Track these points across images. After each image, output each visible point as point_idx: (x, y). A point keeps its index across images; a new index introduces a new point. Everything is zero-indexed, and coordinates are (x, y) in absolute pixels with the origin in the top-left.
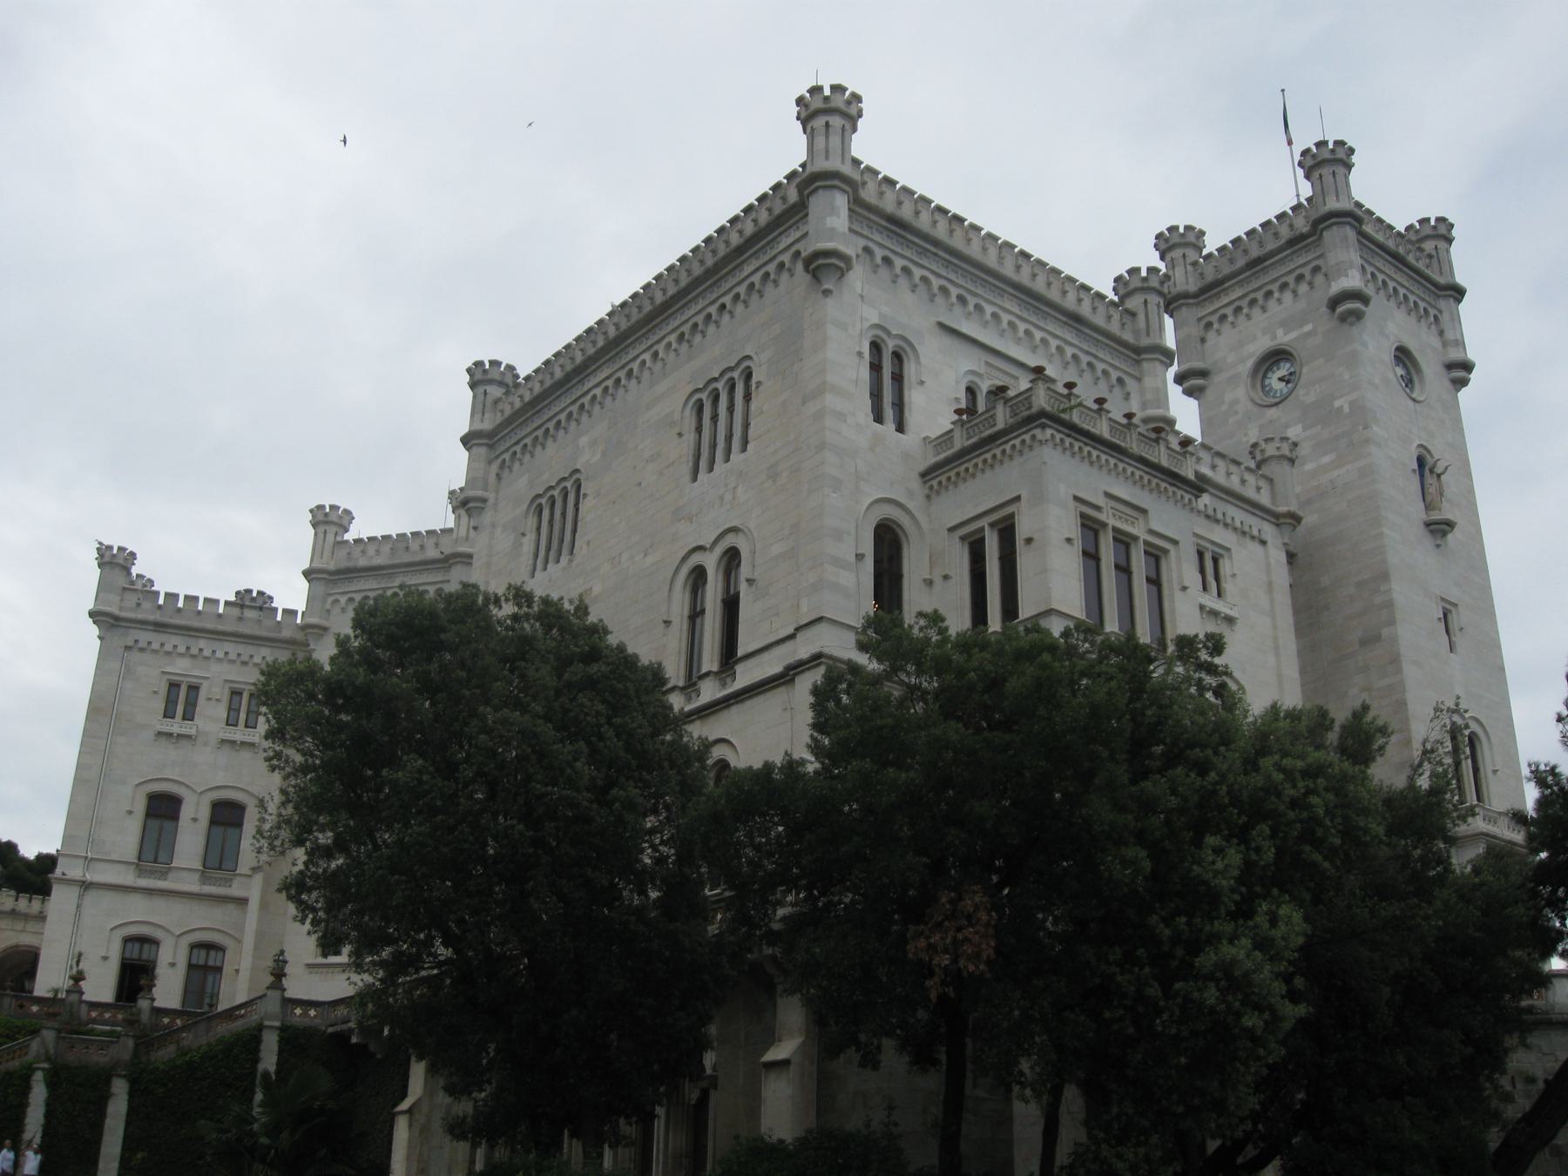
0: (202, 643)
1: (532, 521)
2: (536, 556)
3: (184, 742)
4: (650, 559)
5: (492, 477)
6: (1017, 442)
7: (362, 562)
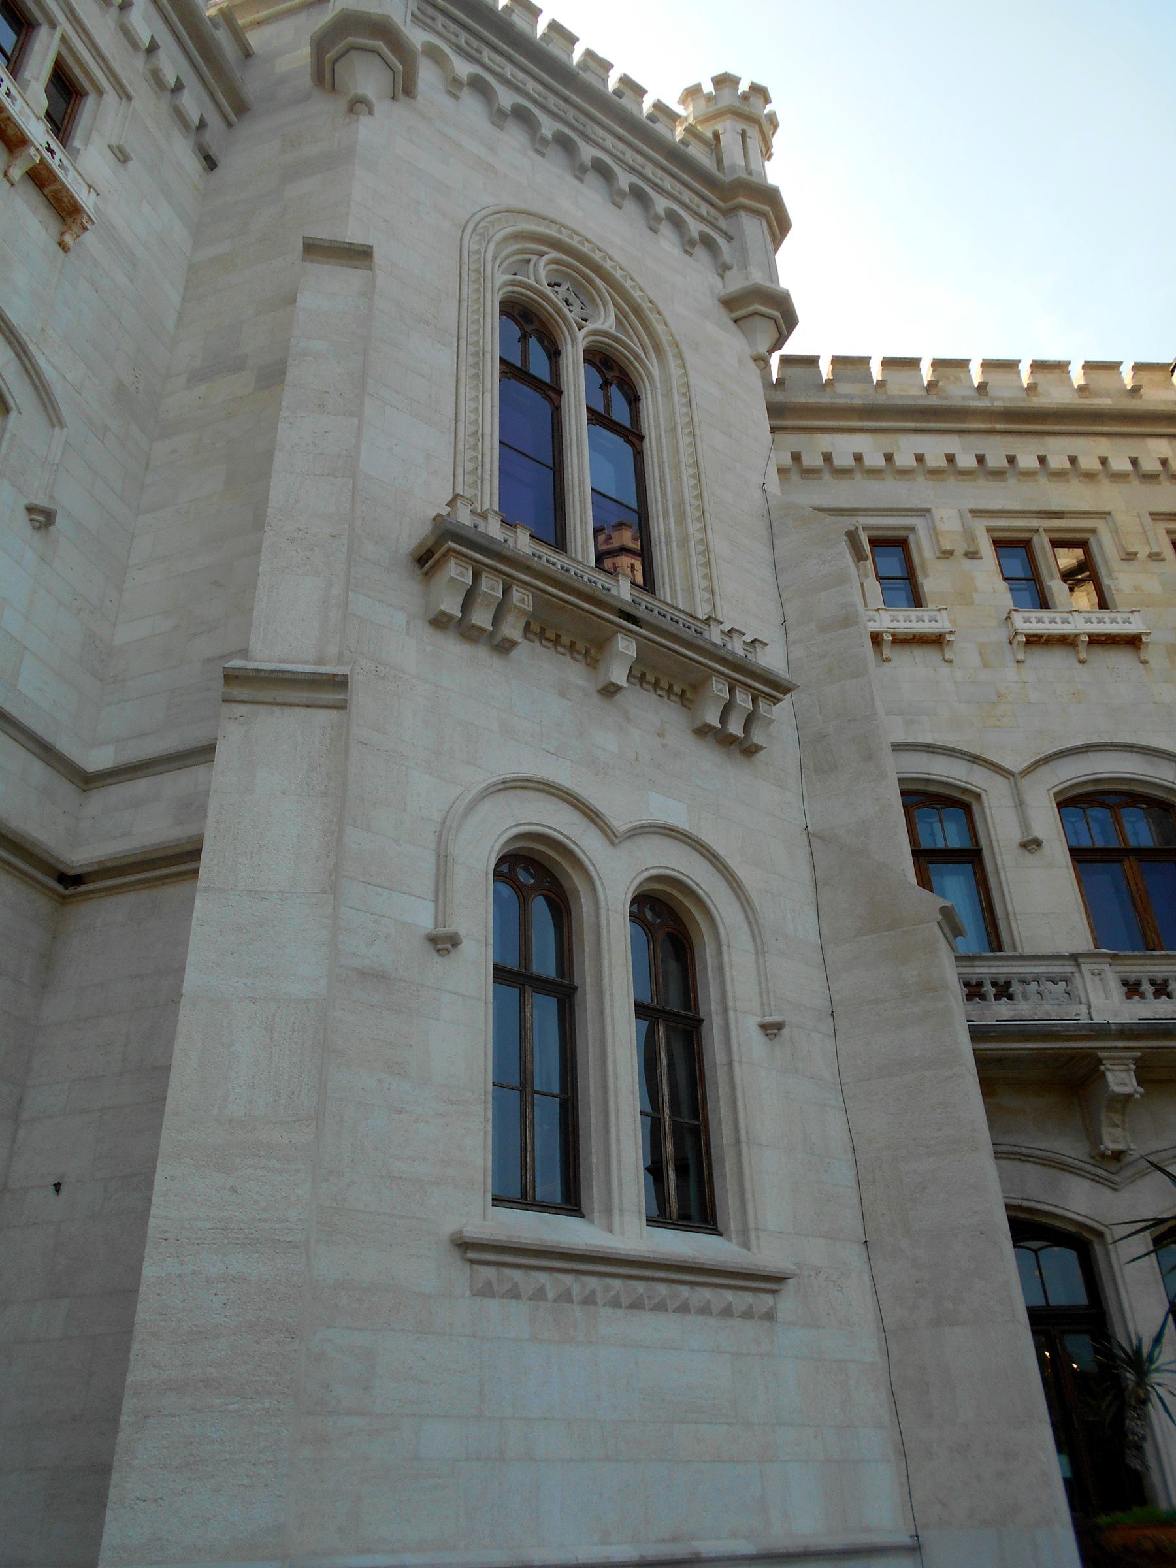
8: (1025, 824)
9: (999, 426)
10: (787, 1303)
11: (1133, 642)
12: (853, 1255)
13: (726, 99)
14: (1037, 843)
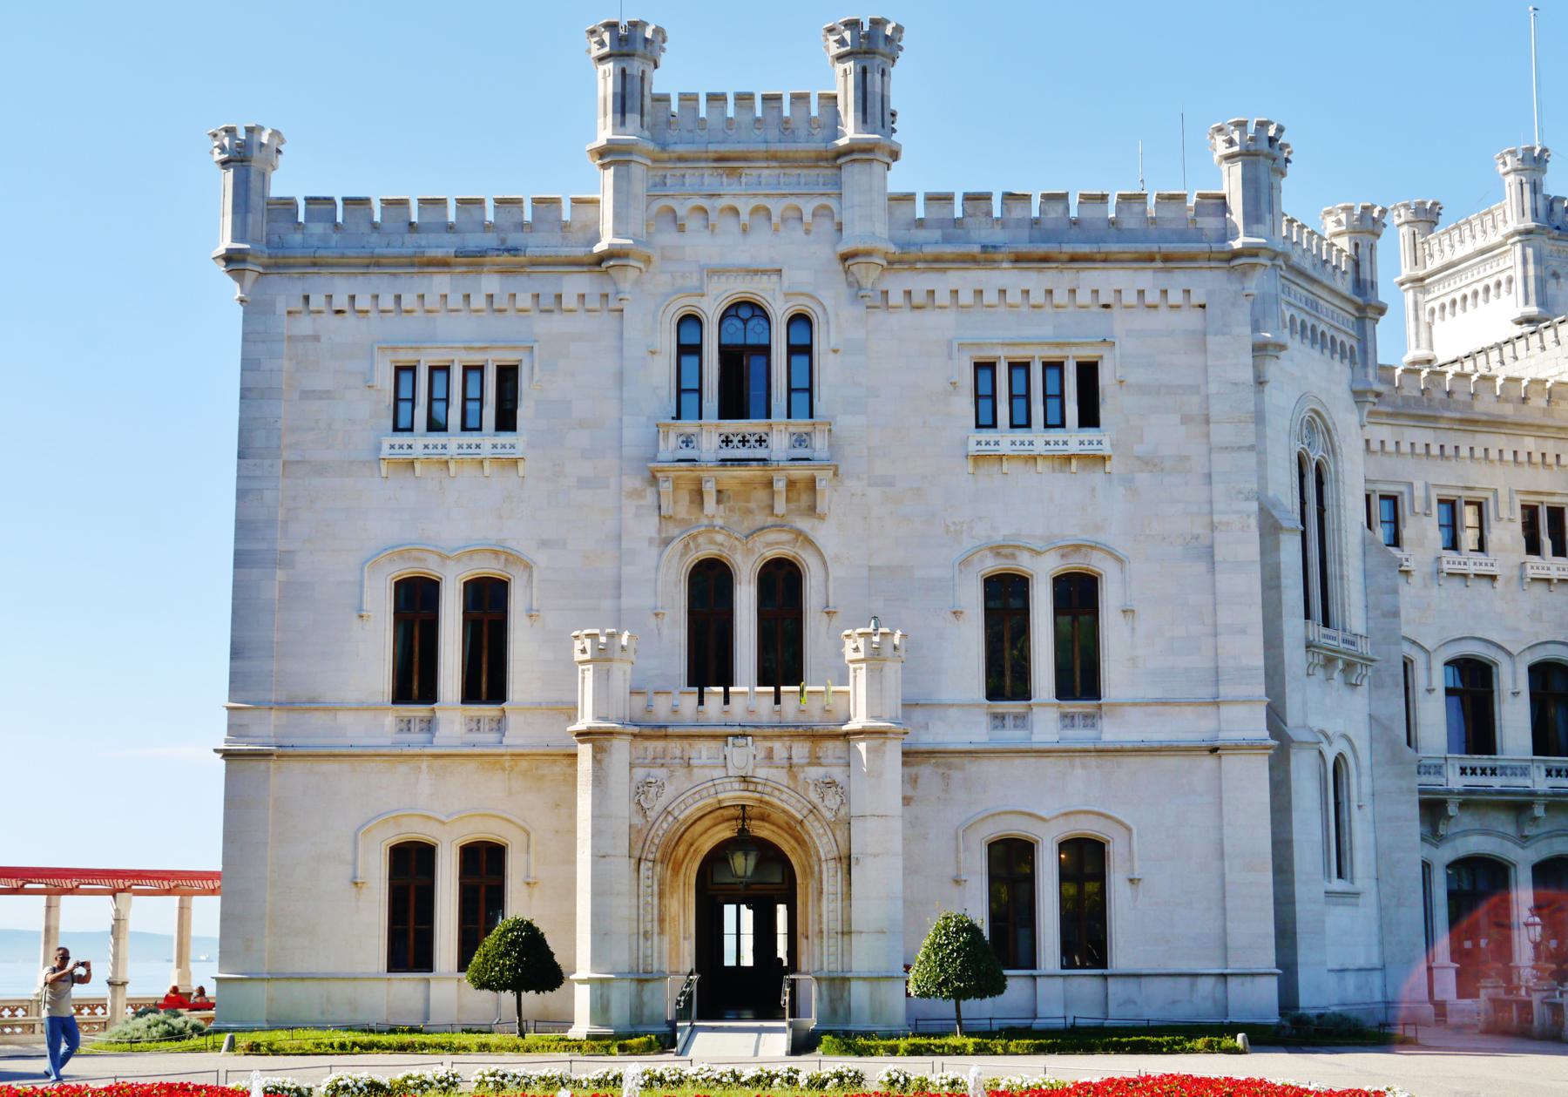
9: (1455, 427)
10: (1361, 900)
11: (1493, 578)
12: (1373, 883)
14: (1433, 690)
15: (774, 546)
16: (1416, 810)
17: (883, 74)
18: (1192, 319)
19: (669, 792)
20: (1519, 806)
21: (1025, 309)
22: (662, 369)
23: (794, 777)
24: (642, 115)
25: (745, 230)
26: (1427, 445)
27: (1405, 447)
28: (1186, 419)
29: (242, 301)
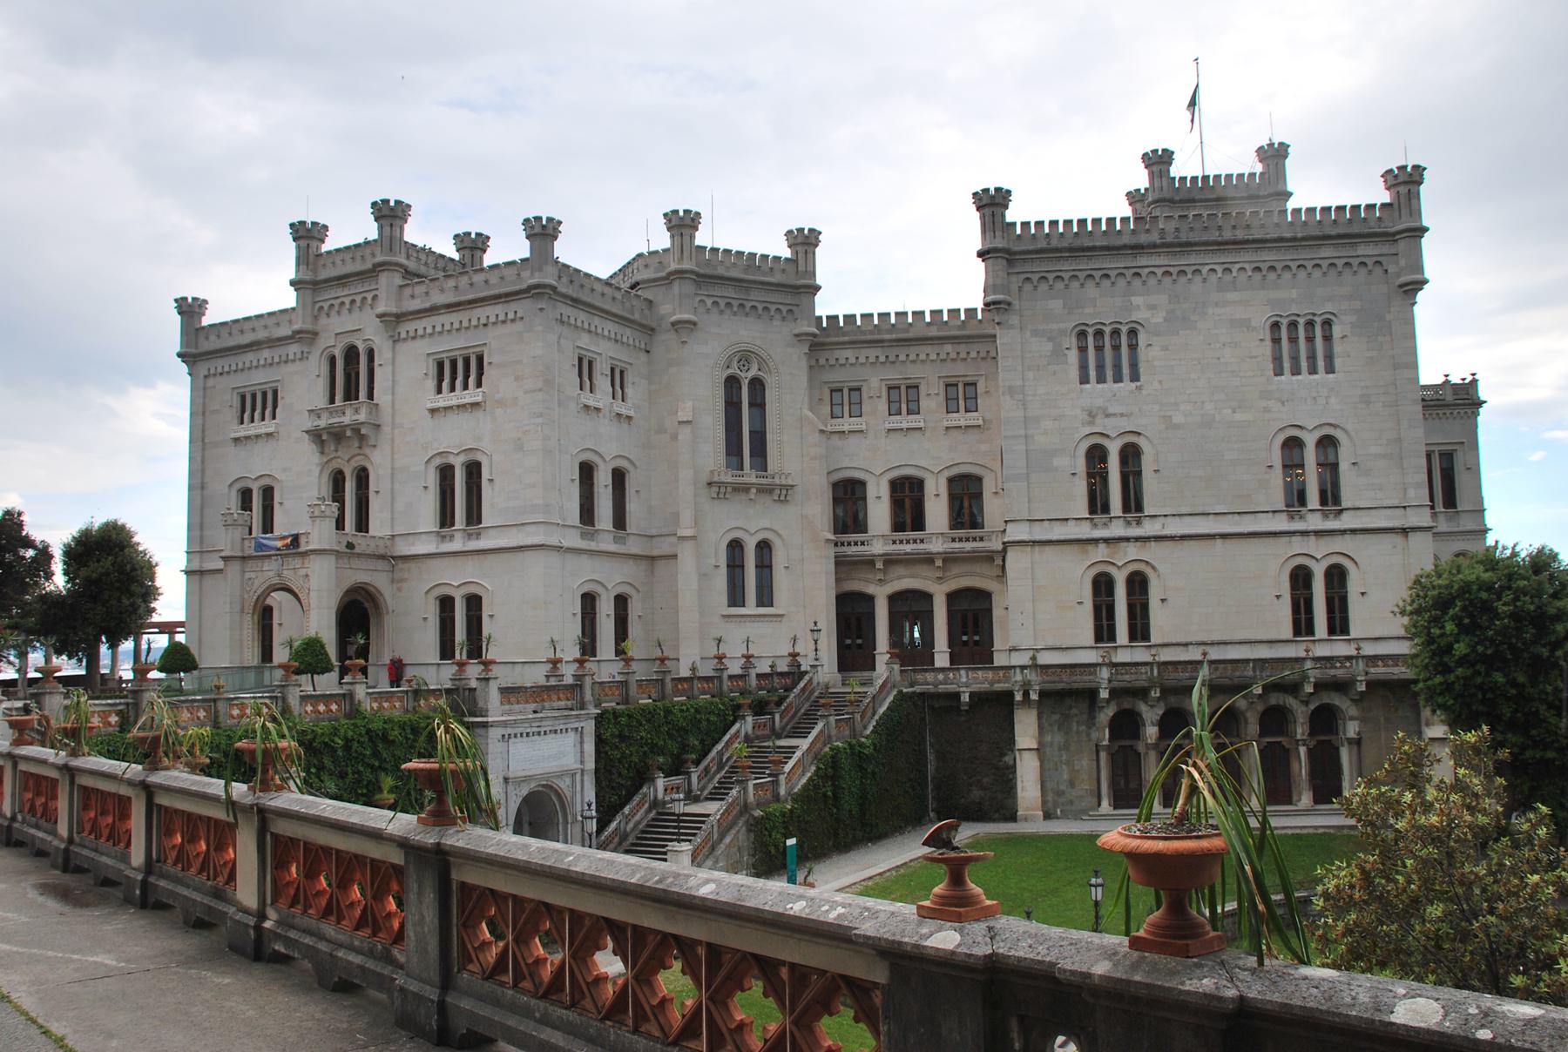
0: (596, 321)
1: (1074, 340)
2: (1083, 368)
3: (594, 414)
4: (1238, 417)
5: (1014, 287)
6: (1462, 411)
7: (721, 271)
8: (879, 492)
10: (784, 619)
13: (800, 240)
15: (358, 461)
16: (832, 567)
17: (391, 225)
18: (519, 326)
19: (257, 583)
20: (928, 559)
21: (454, 332)
22: (322, 385)
23: (295, 573)
24: (308, 265)
25: (350, 311)
26: (877, 357)
27: (862, 360)
28: (517, 379)
29: (190, 374)
